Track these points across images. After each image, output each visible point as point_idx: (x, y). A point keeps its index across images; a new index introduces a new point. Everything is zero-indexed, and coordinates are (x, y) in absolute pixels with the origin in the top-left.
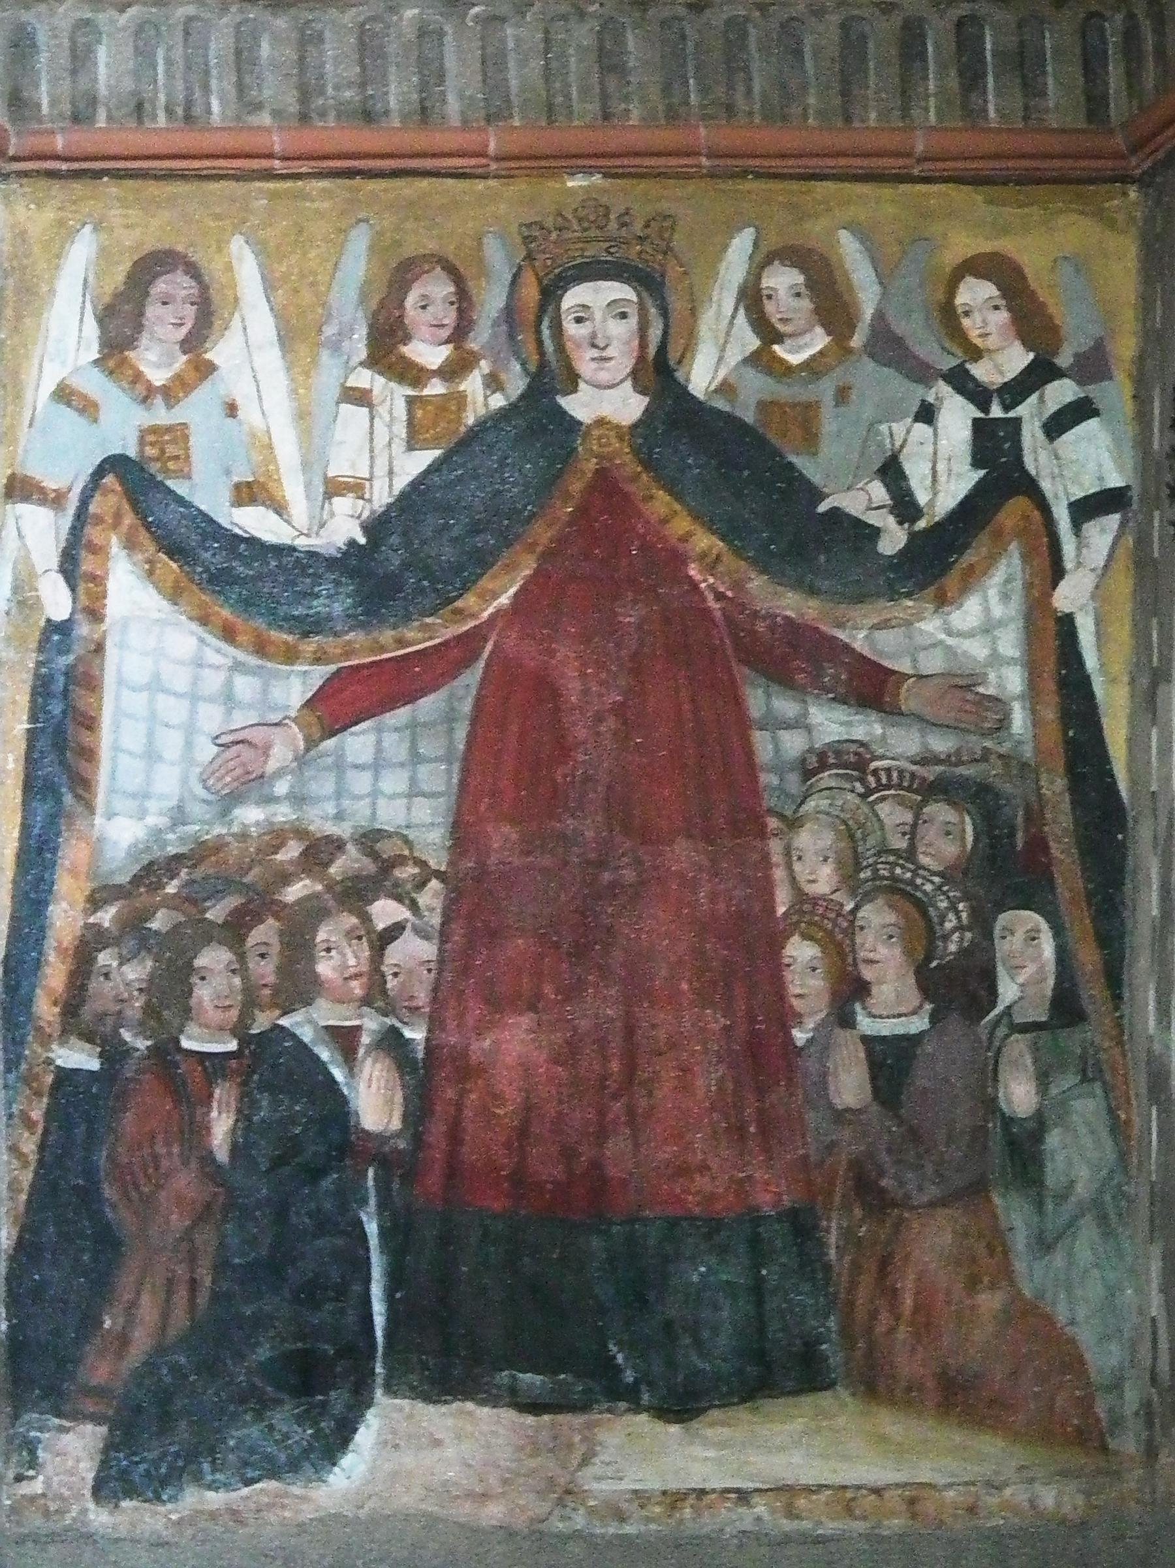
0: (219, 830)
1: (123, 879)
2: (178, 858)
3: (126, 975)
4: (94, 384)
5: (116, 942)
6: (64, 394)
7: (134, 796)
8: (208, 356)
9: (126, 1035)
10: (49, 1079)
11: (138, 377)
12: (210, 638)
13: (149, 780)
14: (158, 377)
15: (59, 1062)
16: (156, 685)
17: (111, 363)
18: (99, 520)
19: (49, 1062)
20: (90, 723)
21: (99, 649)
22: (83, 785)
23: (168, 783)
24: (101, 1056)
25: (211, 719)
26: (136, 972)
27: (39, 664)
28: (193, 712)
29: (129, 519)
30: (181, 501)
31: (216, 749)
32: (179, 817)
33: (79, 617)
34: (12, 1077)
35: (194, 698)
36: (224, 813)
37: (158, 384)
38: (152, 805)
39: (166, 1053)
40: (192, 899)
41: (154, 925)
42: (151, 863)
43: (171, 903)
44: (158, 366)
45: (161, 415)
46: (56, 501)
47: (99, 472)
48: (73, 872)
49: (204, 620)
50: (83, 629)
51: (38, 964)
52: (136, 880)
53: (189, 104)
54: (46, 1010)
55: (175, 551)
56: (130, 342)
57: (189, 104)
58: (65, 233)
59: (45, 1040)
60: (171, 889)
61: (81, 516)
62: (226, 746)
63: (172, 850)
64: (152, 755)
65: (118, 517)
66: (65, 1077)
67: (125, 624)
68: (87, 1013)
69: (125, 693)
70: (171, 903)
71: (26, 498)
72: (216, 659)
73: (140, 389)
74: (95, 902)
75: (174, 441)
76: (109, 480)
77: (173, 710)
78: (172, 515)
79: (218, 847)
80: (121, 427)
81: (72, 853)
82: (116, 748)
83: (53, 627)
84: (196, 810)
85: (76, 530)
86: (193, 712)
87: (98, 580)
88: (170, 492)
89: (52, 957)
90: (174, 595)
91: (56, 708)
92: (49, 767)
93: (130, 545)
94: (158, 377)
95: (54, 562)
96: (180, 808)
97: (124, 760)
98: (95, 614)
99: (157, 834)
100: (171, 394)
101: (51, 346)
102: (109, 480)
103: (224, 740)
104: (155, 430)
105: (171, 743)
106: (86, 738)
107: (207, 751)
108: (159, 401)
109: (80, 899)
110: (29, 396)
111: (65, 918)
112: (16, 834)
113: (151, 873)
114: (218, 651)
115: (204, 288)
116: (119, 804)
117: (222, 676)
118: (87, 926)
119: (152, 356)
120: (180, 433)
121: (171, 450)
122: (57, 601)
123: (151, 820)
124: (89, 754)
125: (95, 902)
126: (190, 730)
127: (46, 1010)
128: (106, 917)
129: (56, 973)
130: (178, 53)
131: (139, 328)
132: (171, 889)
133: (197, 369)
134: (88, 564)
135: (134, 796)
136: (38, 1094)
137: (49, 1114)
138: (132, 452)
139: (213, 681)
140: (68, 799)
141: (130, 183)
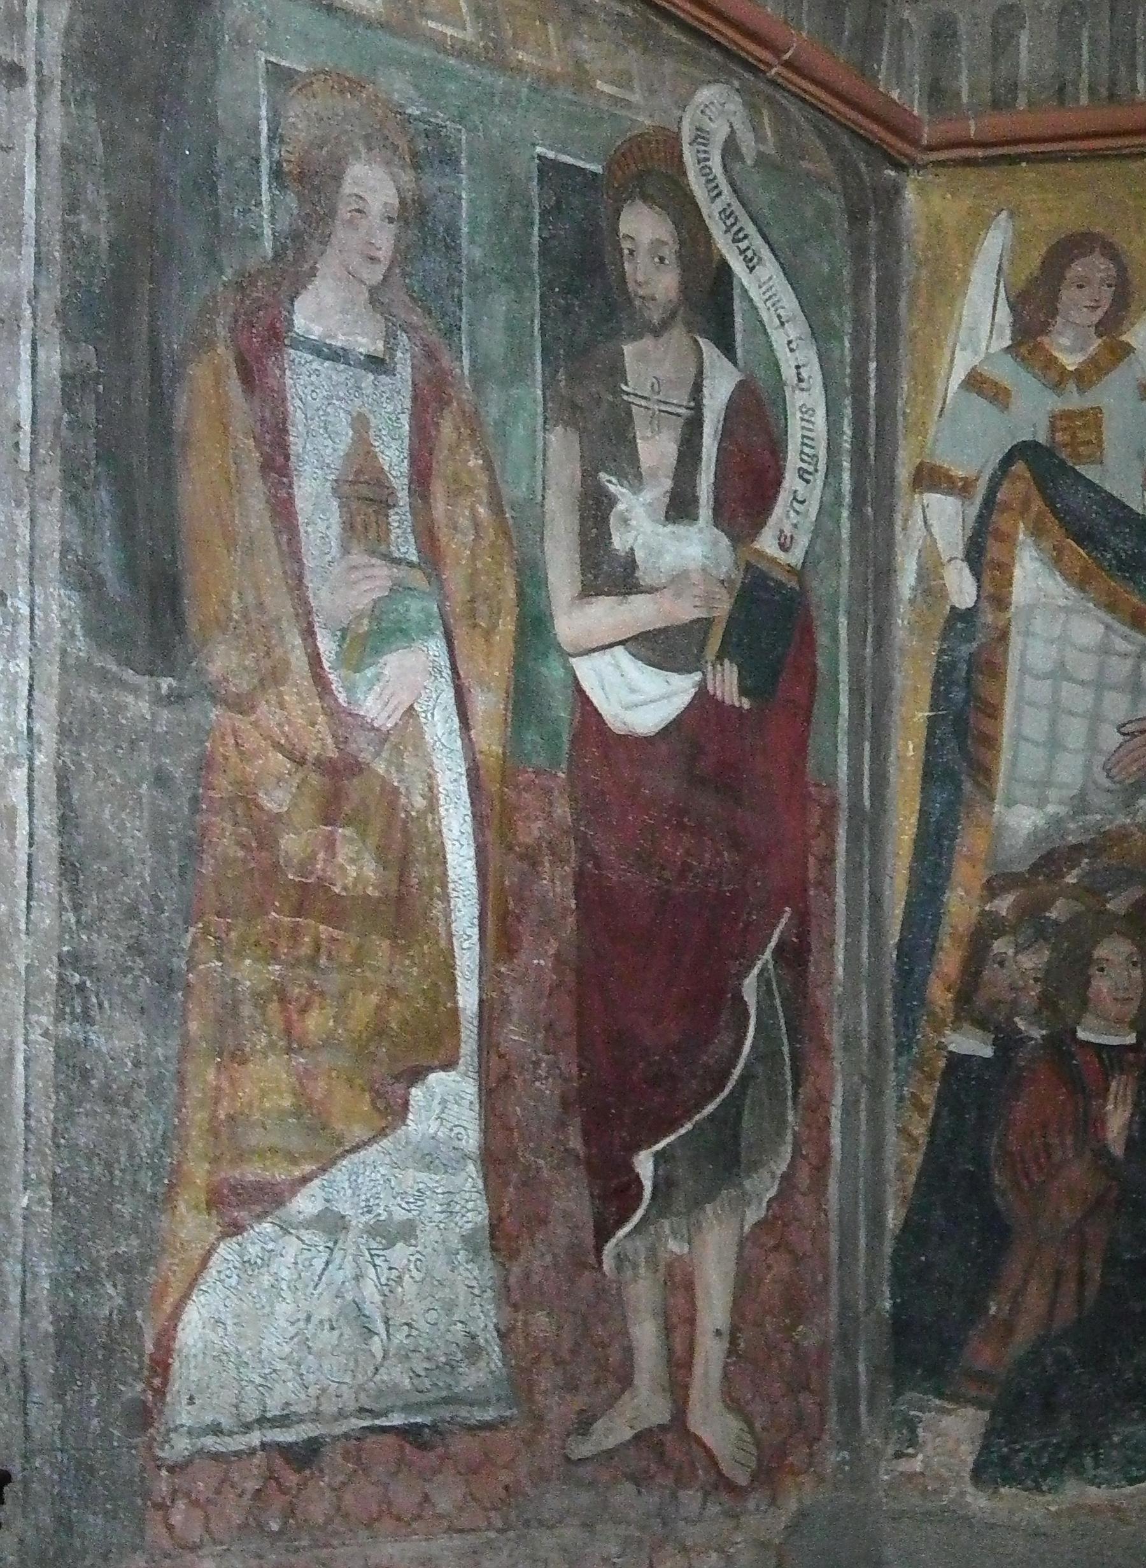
0: (1123, 819)
1: (1022, 868)
2: (1078, 848)
3: (1021, 964)
4: (1006, 372)
5: (1014, 930)
6: (975, 382)
7: (1034, 784)
8: (1124, 338)
9: (1021, 1025)
10: (942, 1064)
11: (1051, 362)
12: (1117, 625)
13: (1050, 769)
14: (1071, 362)
15: (951, 1048)
16: (1060, 673)
17: (1023, 350)
18: (1006, 507)
19: (941, 1047)
20: (993, 712)
21: (1003, 636)
22: (984, 773)
23: (1070, 771)
24: (995, 1042)
25: (1117, 706)
26: (1032, 961)
27: (942, 651)
28: (1099, 700)
29: (1037, 505)
30: (1090, 485)
31: (1121, 739)
32: (1080, 805)
33: (985, 604)
34: (903, 1060)
35: (1099, 686)
36: (1128, 804)
37: (1071, 368)
38: (1052, 793)
39: (1061, 1044)
40: (1093, 890)
41: (1053, 914)
42: (1050, 853)
43: (1072, 893)
44: (1071, 350)
45: (1074, 401)
46: (961, 489)
47: (1008, 460)
48: (972, 859)
49: (1111, 607)
50: (988, 617)
51: (933, 950)
52: (1035, 869)
53: (1113, 83)
54: (940, 996)
55: (1085, 537)
56: (1044, 328)
57: (1113, 83)
58: (981, 222)
59: (938, 1031)
60: (1071, 879)
61: (989, 503)
62: (1132, 735)
63: (1071, 839)
64: (1054, 743)
65: (1026, 503)
66: (957, 1062)
67: (1031, 608)
68: (980, 1001)
69: (1028, 680)
70: (1072, 893)
71: (934, 488)
72: (1121, 645)
73: (1053, 375)
74: (992, 889)
75: (1085, 426)
76: (1019, 467)
77: (1076, 697)
78: (1077, 499)
79: (1123, 835)
80: (1032, 412)
81: (971, 842)
82: (1018, 736)
83: (956, 615)
84: (1098, 799)
85: (983, 519)
86: (1099, 700)
87: (1005, 569)
88: (1079, 476)
89: (947, 943)
90: (1082, 582)
91: (958, 695)
92: (950, 755)
93: (1037, 532)
94: (1071, 362)
95: (959, 551)
96: (1082, 796)
97: (1026, 749)
98: (1001, 602)
99: (1056, 822)
100: (1083, 379)
101: (963, 335)
102: (1019, 467)
103: (1130, 728)
104: (1067, 415)
105: (1075, 732)
106: (986, 726)
107: (1111, 739)
108: (1071, 386)
109: (977, 886)
110: (940, 386)
111: (960, 905)
112: (914, 820)
113: (1051, 861)
114: (1125, 637)
115: (1122, 269)
116: (1018, 791)
117: (1129, 663)
118: (983, 913)
119: (1065, 341)
120: (1093, 418)
121: (1082, 435)
122: (962, 588)
123: (1051, 809)
124: (990, 742)
125: (992, 889)
126: (1095, 718)
127: (940, 996)
128: (1003, 905)
129: (949, 960)
130: (1104, 33)
131: (1054, 313)
132: (1071, 879)
133: (1112, 351)
134: (994, 550)
135: (1034, 784)
136: (930, 1078)
137: (941, 1099)
138: (1042, 439)
139: (1121, 669)
140: (968, 786)
141: (1050, 167)
